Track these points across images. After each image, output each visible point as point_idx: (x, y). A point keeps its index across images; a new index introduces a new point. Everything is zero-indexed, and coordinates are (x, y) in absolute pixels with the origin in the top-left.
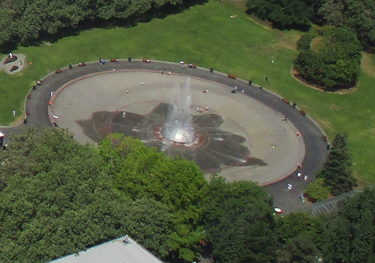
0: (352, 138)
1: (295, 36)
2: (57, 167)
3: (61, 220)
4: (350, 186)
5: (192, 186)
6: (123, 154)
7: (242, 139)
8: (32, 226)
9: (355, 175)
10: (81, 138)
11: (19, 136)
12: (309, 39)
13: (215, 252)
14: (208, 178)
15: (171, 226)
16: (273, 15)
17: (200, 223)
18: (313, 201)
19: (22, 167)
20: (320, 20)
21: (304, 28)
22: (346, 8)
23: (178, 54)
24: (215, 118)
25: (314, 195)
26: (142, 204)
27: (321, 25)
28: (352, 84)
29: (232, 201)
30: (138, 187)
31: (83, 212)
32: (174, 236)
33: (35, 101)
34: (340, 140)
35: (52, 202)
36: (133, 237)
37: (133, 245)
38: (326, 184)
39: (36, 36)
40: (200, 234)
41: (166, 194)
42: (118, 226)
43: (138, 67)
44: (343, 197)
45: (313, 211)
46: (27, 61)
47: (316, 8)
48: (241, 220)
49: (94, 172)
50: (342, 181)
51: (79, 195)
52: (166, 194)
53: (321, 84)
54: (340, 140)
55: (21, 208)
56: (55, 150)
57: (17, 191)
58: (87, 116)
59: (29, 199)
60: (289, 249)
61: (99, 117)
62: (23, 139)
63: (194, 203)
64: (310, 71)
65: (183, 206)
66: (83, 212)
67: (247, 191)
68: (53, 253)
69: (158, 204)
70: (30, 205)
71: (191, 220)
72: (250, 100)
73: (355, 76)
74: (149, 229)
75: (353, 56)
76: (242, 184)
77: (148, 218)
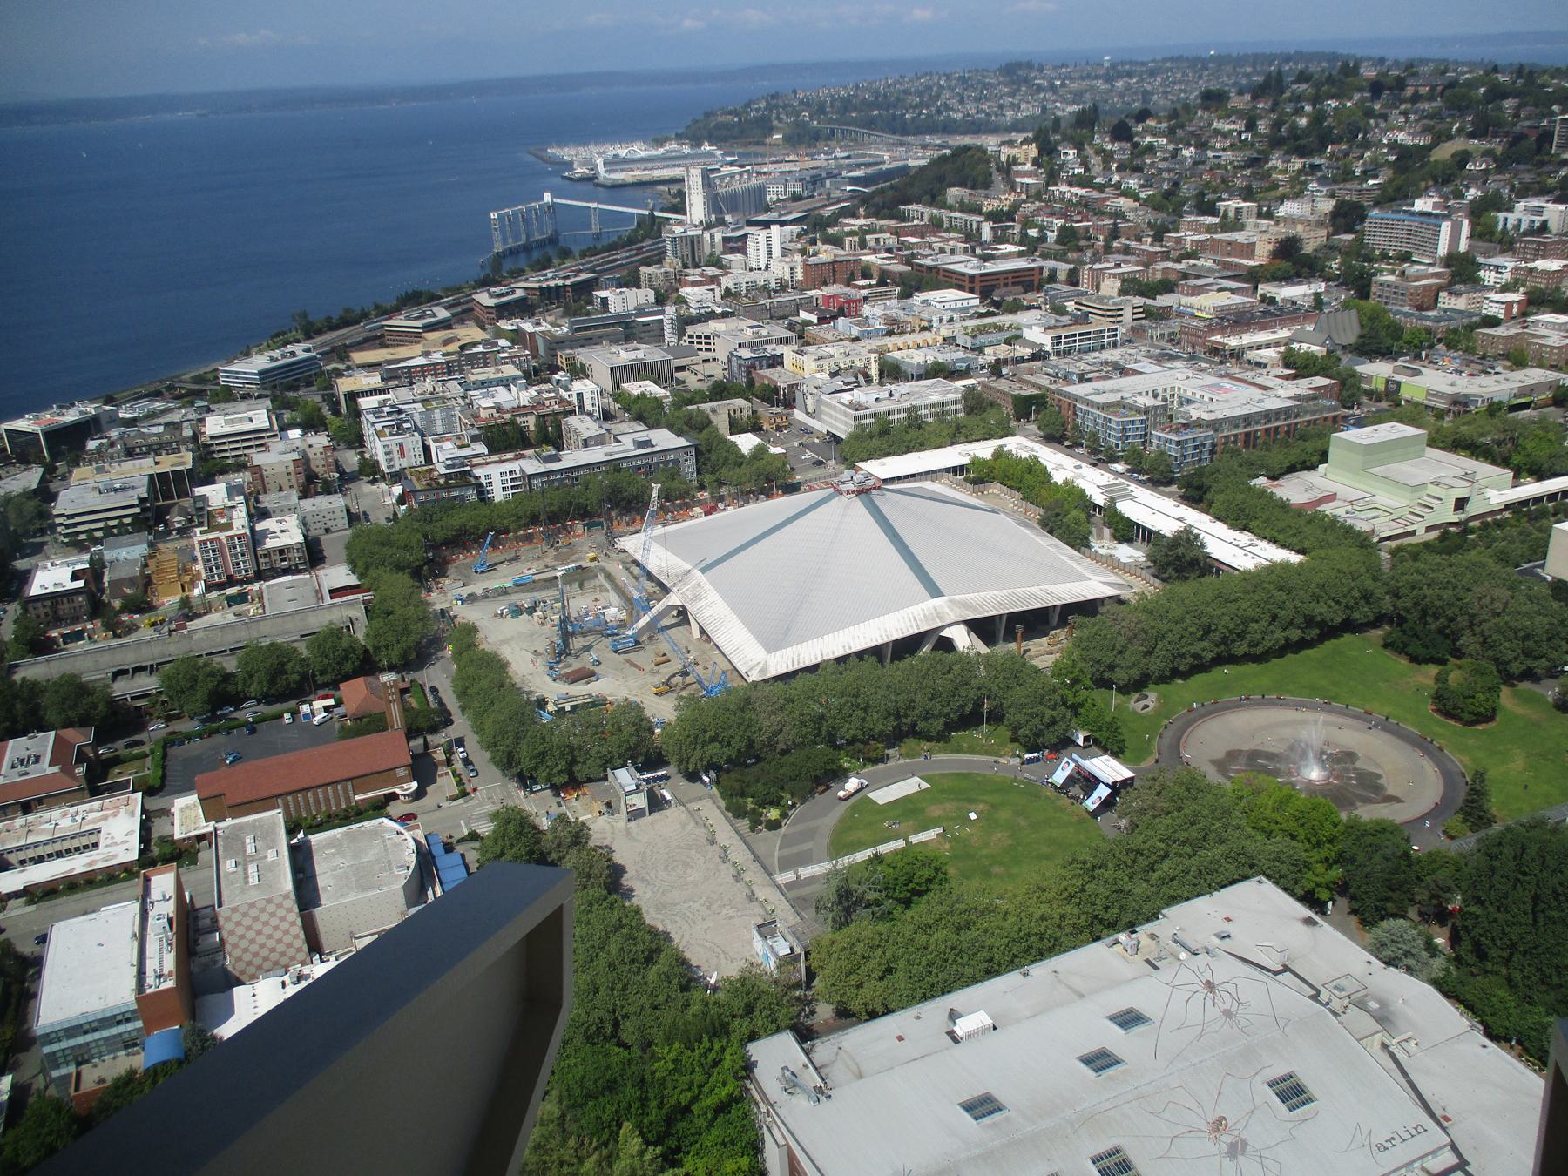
0: (1492, 774)
1: (1433, 670)
3: (1194, 861)
4: (1490, 822)
6: (1257, 792)
7: (1379, 776)
8: (1166, 866)
9: (1494, 811)
10: (1213, 776)
12: (1447, 674)
14: (1344, 816)
15: (1307, 865)
16: (1410, 649)
17: (1336, 862)
18: (1452, 838)
19: (1153, 807)
20: (1458, 654)
22: (1485, 641)
23: (1313, 690)
24: (1350, 756)
25: (1453, 833)
26: (1278, 843)
27: (1459, 658)
28: (1492, 719)
29: (1369, 839)
30: (1273, 826)
31: (1216, 852)
32: (1309, 875)
33: (1166, 740)
34: (1479, 776)
35: (1184, 843)
36: (1268, 877)
37: (1269, 888)
38: (1465, 821)
39: (1168, 673)
40: (1336, 873)
43: (1272, 704)
44: (1482, 834)
46: (1158, 699)
47: (1455, 640)
48: (1377, 858)
49: (1227, 812)
50: (1481, 818)
51: (1212, 835)
52: (1302, 833)
53: (1459, 719)
54: (1479, 776)
55: (1153, 850)
56: (1188, 790)
57: (1149, 833)
58: (1220, 755)
60: (1427, 887)
61: (1232, 755)
62: (1154, 779)
63: (1330, 841)
64: (1447, 706)
65: (1319, 844)
66: (1216, 852)
67: (1382, 829)
68: (1186, 894)
69: (1294, 843)
70: (1162, 846)
71: (1327, 859)
72: (1385, 736)
73: (1494, 710)
74: (1284, 869)
75: (1493, 690)
76: (1378, 822)
77: (1283, 857)
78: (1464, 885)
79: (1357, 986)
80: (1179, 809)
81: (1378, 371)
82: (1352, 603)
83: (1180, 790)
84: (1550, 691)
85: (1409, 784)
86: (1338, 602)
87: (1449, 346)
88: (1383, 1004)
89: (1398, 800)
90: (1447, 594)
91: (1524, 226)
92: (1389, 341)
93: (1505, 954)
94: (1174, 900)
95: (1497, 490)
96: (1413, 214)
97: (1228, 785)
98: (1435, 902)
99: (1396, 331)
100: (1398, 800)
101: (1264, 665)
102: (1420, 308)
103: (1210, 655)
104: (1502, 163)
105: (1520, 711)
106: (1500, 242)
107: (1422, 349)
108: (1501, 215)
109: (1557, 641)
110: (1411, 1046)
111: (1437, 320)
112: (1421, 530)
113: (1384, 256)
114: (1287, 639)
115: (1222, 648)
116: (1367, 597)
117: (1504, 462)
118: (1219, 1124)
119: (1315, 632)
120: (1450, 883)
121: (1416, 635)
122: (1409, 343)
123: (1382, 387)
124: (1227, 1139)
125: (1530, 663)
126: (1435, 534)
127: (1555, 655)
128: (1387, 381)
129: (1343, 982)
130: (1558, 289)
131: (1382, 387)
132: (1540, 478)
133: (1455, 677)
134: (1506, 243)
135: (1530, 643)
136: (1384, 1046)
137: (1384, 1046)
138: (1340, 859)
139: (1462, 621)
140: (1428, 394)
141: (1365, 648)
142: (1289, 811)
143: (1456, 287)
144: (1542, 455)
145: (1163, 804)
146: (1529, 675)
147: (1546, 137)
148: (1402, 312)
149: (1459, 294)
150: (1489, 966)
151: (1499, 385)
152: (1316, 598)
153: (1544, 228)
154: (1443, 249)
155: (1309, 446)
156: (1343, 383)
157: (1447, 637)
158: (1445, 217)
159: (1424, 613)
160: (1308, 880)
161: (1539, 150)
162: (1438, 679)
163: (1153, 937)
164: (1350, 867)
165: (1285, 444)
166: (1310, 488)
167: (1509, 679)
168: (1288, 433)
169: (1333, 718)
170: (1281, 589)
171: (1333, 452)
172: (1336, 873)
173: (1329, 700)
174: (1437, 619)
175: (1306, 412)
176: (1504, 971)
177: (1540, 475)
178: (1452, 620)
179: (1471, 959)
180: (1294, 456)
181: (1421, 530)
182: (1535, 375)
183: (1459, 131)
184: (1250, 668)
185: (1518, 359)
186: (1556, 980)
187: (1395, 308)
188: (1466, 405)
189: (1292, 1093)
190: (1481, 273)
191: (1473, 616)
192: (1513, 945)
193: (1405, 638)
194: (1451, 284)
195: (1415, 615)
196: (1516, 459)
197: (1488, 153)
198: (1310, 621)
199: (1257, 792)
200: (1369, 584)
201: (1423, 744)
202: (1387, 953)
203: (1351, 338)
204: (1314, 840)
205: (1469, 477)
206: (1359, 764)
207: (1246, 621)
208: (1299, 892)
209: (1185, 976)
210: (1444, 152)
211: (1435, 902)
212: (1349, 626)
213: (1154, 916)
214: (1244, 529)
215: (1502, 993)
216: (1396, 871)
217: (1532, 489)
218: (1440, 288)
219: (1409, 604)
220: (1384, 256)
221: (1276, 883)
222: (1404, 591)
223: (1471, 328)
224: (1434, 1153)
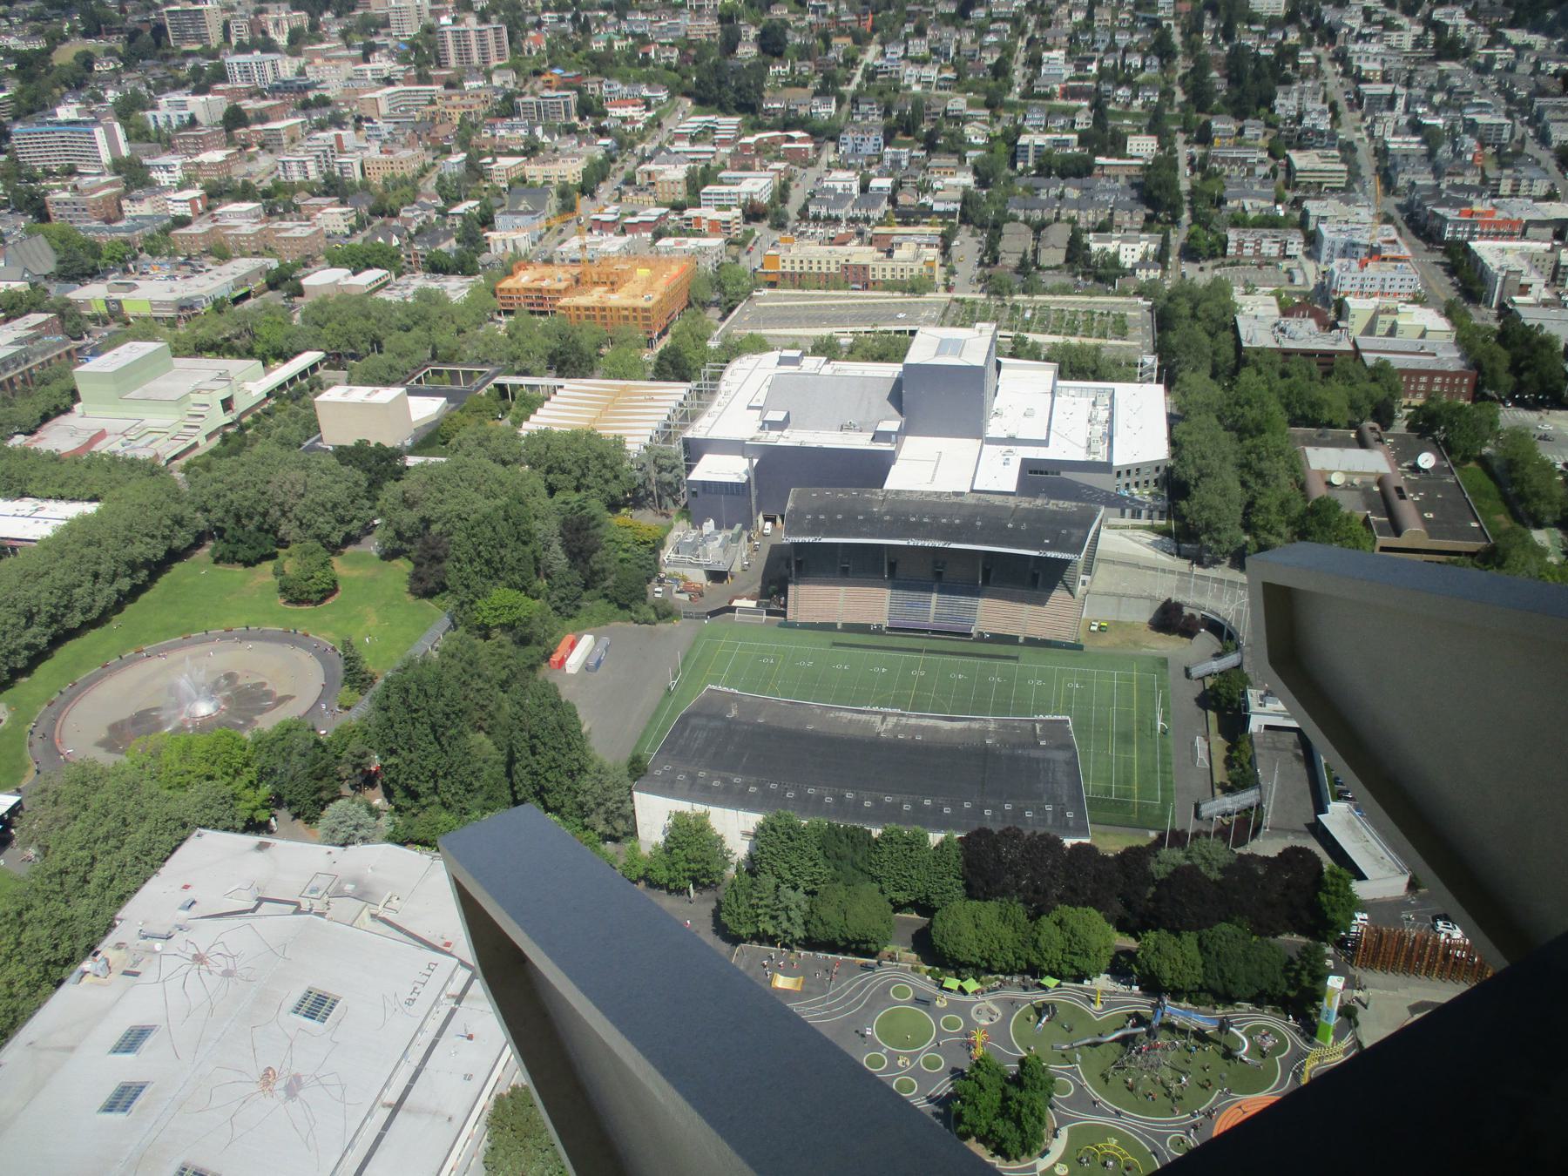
1: (268, 566)
2: (95, 802)
3: (125, 850)
4: (372, 680)
5: (236, 751)
6: (156, 754)
7: (264, 684)
9: (372, 669)
10: (106, 759)
11: (39, 789)
12: (282, 565)
13: (286, 798)
14: (247, 735)
16: (240, 556)
17: (260, 781)
18: (348, 708)
21: (273, 556)
23: (168, 630)
25: (346, 704)
26: (198, 792)
28: (333, 590)
32: (242, 805)
34: (347, 644)
35: (106, 838)
36: (204, 827)
37: (208, 833)
38: (352, 688)
41: (217, 770)
42: (184, 826)
44: (371, 693)
45: (352, 718)
47: (275, 533)
48: (295, 758)
52: (217, 771)
53: (310, 602)
54: (347, 644)
55: (75, 863)
56: (84, 784)
57: (63, 847)
58: (104, 734)
59: (82, 848)
61: (115, 728)
62: (44, 791)
63: (247, 765)
64: (296, 595)
65: (237, 772)
67: (288, 730)
73: (334, 582)
74: (215, 813)
78: (375, 744)
79: (329, 879)
80: (85, 808)
81: (92, 294)
82: (167, 532)
83: (79, 789)
84: (371, 546)
85: (292, 680)
86: (153, 537)
87: (151, 253)
88: (356, 881)
89: (291, 697)
90: (251, 493)
91: (175, 122)
92: (91, 261)
93: (431, 785)
94: (122, 899)
95: (255, 382)
96: (59, 124)
97: (124, 760)
98: (359, 771)
99: (95, 250)
100: (291, 697)
101: (107, 626)
102: (108, 221)
103: (45, 640)
104: (130, 60)
105: (355, 573)
106: (159, 141)
107: (126, 261)
108: (149, 114)
109: (359, 502)
110: (395, 903)
111: (130, 230)
112: (202, 441)
113: (48, 173)
114: (119, 591)
115: (55, 626)
116: (179, 522)
117: (250, 353)
118: (268, 1076)
119: (144, 574)
120: (365, 748)
121: (239, 541)
122: (112, 258)
123: (103, 310)
124: (281, 1084)
125: (346, 528)
126: (217, 440)
127: (361, 514)
128: (107, 302)
129: (315, 883)
130: (230, 178)
131: (103, 310)
132: (286, 360)
133: (290, 564)
134: (166, 142)
135: (340, 511)
136: (374, 916)
137: (374, 916)
138: (265, 775)
139: (275, 512)
140: (152, 306)
141: (198, 570)
142: (197, 754)
143: (135, 193)
144: (278, 338)
145: (65, 810)
146: (349, 540)
147: (159, 30)
148: (90, 228)
149: (140, 200)
150: (423, 801)
151: (214, 282)
152: (129, 541)
153: (193, 122)
154: (106, 158)
155: (55, 388)
156: (61, 315)
157: (267, 531)
158: (96, 122)
159: (238, 518)
160: (243, 810)
161: (158, 44)
162: (276, 574)
163: (119, 946)
164: (274, 778)
165: (28, 394)
166: (74, 433)
167: (335, 549)
168: (24, 381)
169: (198, 649)
170: (90, 544)
171: (81, 389)
172: (266, 790)
173: (185, 633)
174: (251, 518)
175: (35, 355)
176: (436, 799)
177: (284, 356)
178: (265, 514)
179: (407, 803)
180: (42, 403)
181: (202, 441)
182: (243, 266)
183: (73, 30)
184: (93, 635)
185: (223, 255)
186: (477, 785)
187: (82, 225)
188: (192, 308)
189: (317, 1006)
190: (154, 175)
191: (281, 505)
192: (434, 775)
193: (231, 547)
194: (128, 190)
195: (230, 523)
196: (259, 348)
197: (110, 52)
198: (133, 566)
199: (156, 754)
200: (175, 509)
201: (289, 637)
202: (340, 836)
203: (49, 265)
204: (231, 771)
205: (224, 377)
206: (240, 682)
207: (68, 590)
208: (241, 825)
209: (170, 964)
210: (65, 55)
211: (359, 771)
212: (174, 556)
213: (110, 926)
214: (23, 495)
215: (444, 816)
216: (315, 761)
217: (283, 372)
218: (119, 197)
219: (220, 514)
220: (48, 173)
221: (215, 828)
222: (210, 504)
223: (166, 231)
224: (451, 978)
